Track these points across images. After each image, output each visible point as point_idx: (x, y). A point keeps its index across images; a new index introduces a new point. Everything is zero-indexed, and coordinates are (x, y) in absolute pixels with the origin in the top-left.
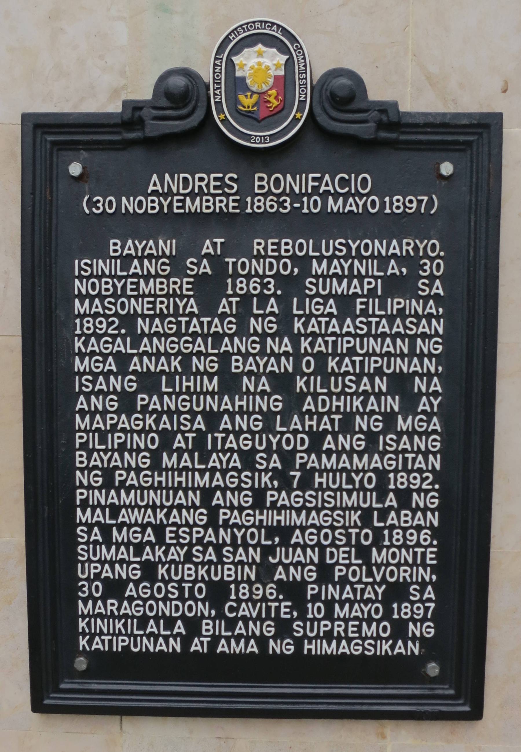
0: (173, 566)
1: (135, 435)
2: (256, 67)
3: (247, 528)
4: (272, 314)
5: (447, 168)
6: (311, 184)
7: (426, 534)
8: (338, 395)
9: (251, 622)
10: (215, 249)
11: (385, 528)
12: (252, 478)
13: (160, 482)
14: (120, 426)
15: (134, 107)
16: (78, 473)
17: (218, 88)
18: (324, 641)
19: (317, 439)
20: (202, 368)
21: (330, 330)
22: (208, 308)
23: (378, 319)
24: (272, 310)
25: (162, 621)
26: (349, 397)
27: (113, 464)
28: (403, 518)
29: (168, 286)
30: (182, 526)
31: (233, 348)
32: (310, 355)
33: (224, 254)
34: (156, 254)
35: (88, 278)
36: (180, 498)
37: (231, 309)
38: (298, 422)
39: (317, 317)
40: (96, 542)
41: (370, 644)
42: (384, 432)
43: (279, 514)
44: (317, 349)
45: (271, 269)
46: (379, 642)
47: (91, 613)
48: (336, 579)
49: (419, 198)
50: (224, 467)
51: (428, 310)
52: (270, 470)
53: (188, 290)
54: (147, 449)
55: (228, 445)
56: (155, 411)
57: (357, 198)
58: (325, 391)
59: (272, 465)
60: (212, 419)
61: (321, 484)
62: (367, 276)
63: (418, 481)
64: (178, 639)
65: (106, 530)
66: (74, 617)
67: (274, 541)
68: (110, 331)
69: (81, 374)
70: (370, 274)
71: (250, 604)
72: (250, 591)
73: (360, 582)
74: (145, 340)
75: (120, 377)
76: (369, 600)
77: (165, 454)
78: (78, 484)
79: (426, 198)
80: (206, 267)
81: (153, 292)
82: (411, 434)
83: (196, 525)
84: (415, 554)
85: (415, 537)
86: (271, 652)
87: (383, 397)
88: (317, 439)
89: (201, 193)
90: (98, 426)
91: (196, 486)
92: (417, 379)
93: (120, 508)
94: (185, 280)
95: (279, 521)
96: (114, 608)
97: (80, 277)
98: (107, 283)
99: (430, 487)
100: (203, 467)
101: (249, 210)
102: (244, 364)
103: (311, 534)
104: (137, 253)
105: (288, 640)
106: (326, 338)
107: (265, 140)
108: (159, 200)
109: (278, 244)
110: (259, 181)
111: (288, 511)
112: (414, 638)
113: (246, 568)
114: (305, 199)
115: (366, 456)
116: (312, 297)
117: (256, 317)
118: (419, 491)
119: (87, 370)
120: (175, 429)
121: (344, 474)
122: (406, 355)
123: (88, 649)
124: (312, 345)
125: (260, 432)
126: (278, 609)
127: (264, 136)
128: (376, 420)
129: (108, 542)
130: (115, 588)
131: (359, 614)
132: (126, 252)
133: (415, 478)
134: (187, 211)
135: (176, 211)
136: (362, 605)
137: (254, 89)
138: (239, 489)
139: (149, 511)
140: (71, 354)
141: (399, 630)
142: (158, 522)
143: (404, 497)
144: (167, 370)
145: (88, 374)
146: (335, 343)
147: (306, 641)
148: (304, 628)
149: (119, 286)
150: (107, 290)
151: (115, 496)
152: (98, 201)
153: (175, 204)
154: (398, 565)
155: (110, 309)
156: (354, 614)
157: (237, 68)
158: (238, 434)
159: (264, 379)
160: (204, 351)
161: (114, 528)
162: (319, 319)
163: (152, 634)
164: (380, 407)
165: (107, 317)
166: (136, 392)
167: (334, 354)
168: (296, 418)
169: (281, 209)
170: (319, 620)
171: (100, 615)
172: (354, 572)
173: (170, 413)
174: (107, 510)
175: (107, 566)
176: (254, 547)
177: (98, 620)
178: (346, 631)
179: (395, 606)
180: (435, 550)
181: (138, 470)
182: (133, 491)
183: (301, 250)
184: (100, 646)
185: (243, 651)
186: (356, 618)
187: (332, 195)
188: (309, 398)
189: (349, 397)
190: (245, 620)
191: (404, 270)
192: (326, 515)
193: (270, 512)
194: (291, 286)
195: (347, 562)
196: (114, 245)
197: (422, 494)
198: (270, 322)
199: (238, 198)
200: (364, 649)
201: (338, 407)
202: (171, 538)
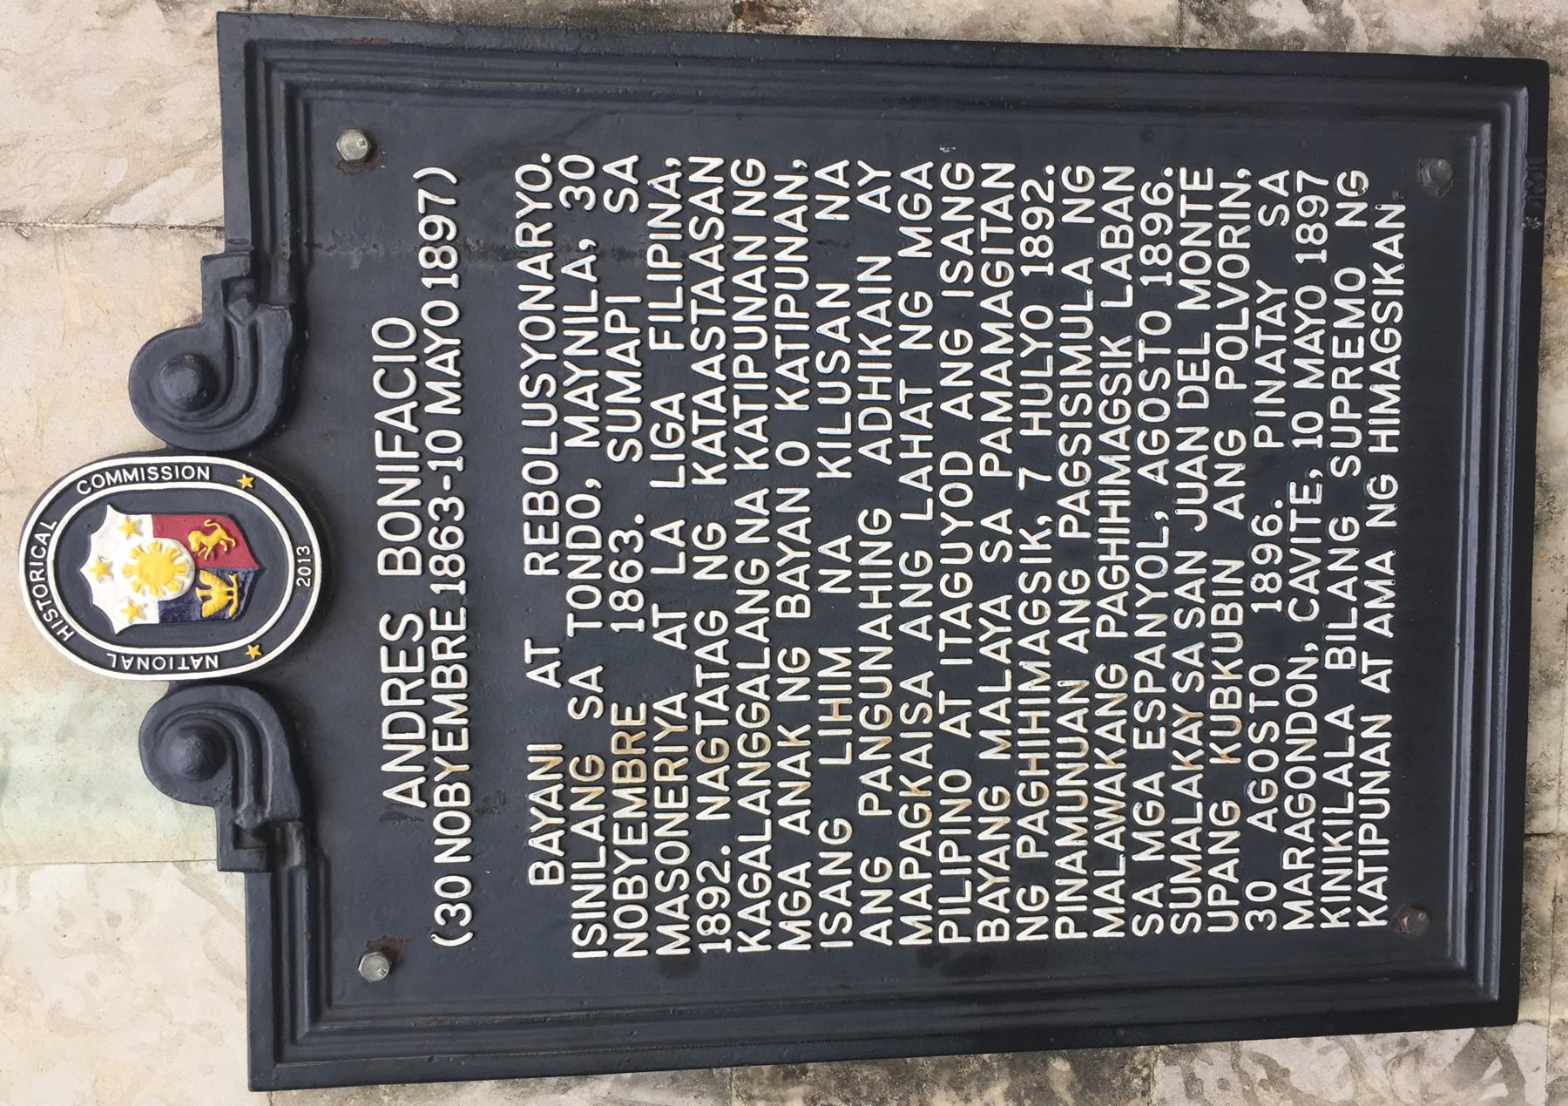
0: (1213, 733)
1: (943, 819)
2: (135, 577)
3: (1135, 578)
4: (685, 534)
5: (352, 145)
6: (397, 453)
8: (858, 388)
9: (1331, 568)
10: (549, 659)
12: (1032, 570)
13: (1041, 764)
14: (923, 851)
16: (1022, 937)
17: (188, 663)
18: (1372, 410)
19: (949, 434)
20: (804, 681)
21: (718, 407)
22: (675, 671)
23: (694, 302)
24: (676, 533)
25: (1327, 755)
26: (861, 366)
27: (1002, 865)
28: (1117, 245)
29: (627, 758)
30: (1130, 717)
31: (760, 616)
33: (559, 640)
34: (560, 787)
35: (612, 929)
36: (1071, 720)
37: (676, 622)
39: (689, 437)
40: (1165, 896)
41: (1381, 313)
44: (759, 436)
45: (589, 538)
46: (1376, 292)
47: (1310, 903)
48: (1243, 386)
49: (421, 209)
50: (1008, 629)
52: (1015, 530)
53: (635, 716)
54: (971, 794)
55: (963, 623)
56: (892, 779)
57: (427, 350)
58: (848, 416)
60: (908, 656)
61: (1043, 424)
62: (599, 327)
63: (1038, 211)
64: (1363, 719)
65: (1139, 876)
66: (1317, 938)
67: (1163, 522)
68: (726, 880)
70: (594, 320)
71: (1293, 570)
73: (1248, 336)
75: (823, 855)
76: (1288, 315)
77: (983, 756)
78: (1045, 937)
79: (422, 194)
80: (588, 678)
81: (643, 790)
82: (941, 230)
83: (1128, 688)
84: (1192, 216)
85: (1157, 217)
86: (1393, 524)
87: (861, 290)
88: (949, 434)
89: (425, 692)
91: (1047, 688)
92: (821, 215)
93: (1094, 849)
94: (614, 722)
95: (1121, 512)
96: (1300, 855)
97: (611, 946)
98: (623, 889)
99: (1051, 184)
100: (1008, 674)
101: (461, 588)
102: (793, 591)
103: (1147, 443)
105: (1370, 487)
106: (737, 415)
107: (304, 555)
108: (442, 782)
109: (534, 522)
110: (395, 568)
111: (1101, 493)
112: (1371, 215)
114: (433, 465)
115: (984, 326)
116: (649, 448)
117: (692, 567)
118: (1058, 209)
119: (808, 923)
120: (929, 735)
121: (1024, 373)
122: (770, 240)
123: (1385, 908)
124: (750, 445)
126: (1303, 511)
128: (909, 304)
129: (1162, 871)
130: (1259, 854)
131: (1316, 335)
132: (555, 850)
134: (464, 721)
136: (1297, 331)
137: (188, 582)
138: (1054, 597)
141: (1352, 248)
142: (1123, 766)
143: (1072, 242)
145: (815, 921)
146: (746, 397)
147: (1372, 449)
148: (1344, 453)
149: (629, 862)
150: (637, 888)
151: (1068, 859)
152: (445, 914)
153: (450, 747)
154: (1215, 253)
155: (679, 879)
157: (138, 621)
158: (942, 603)
159: (824, 549)
160: (767, 677)
161: (1136, 858)
162: (695, 431)
163: (1353, 775)
164: (882, 298)
167: (770, 398)
169: (457, 518)
170: (1329, 422)
171: (1315, 885)
173: (897, 747)
174: (1097, 873)
176: (1175, 562)
177: (1324, 888)
178: (1351, 364)
179: (1300, 258)
180: (1183, 172)
181: (1016, 811)
182: (1059, 821)
183: (545, 473)
184: (1379, 882)
185: (1389, 582)
186: (1326, 343)
187: (421, 405)
188: (864, 451)
189: (861, 366)
190: (1325, 579)
191: (584, 244)
193: (1102, 530)
194: (626, 493)
195: (1206, 363)
197: (1066, 202)
198: (702, 537)
199: (433, 612)
201: (882, 388)
202: (1156, 740)
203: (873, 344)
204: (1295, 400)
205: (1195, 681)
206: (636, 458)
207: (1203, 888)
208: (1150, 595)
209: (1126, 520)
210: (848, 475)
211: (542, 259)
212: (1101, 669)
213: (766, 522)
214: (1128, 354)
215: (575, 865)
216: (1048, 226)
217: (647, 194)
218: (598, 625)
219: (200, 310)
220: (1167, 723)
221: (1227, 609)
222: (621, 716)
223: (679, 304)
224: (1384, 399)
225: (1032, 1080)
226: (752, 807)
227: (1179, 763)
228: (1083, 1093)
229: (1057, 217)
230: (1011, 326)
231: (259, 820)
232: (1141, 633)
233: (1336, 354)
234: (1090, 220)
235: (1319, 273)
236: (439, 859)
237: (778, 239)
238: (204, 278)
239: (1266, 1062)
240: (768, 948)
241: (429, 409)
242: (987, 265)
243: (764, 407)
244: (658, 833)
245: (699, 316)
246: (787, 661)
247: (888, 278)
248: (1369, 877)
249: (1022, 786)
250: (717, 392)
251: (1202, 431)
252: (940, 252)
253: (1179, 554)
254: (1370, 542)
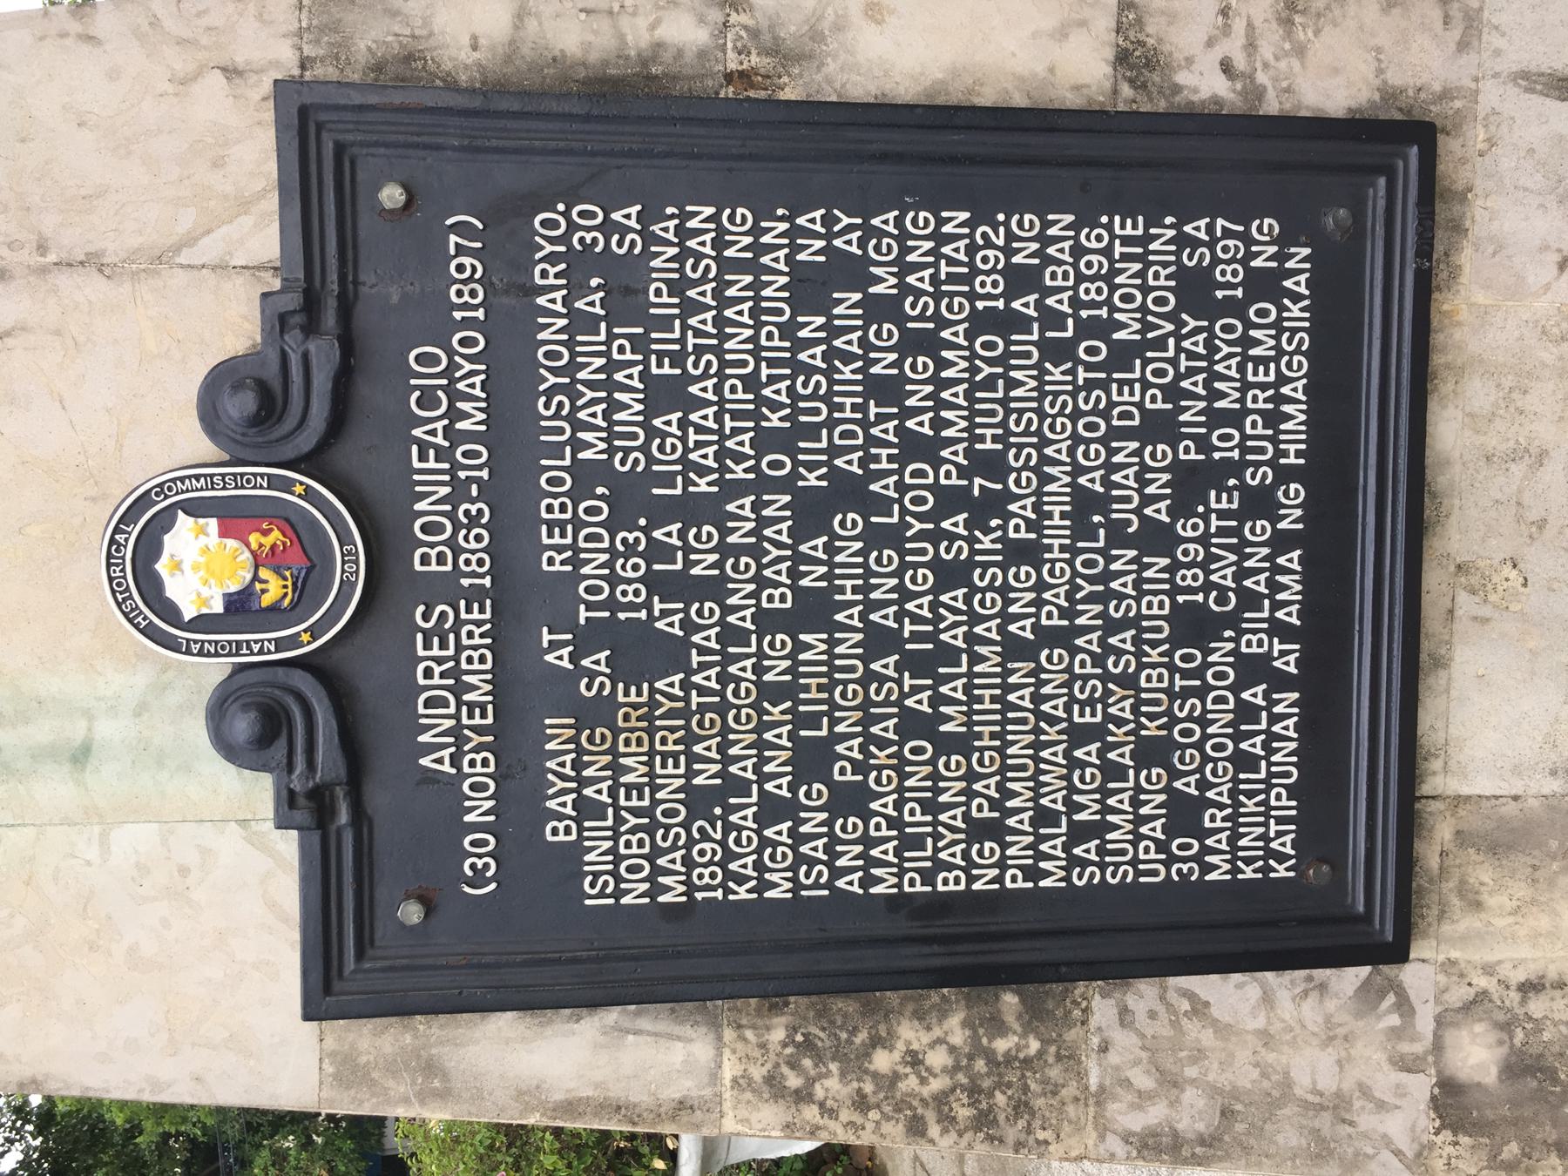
0: (1144, 709)
1: (908, 783)
2: (202, 573)
4: (682, 535)
5: (392, 195)
6: (432, 464)
7: (1088, 237)
8: (833, 407)
9: (1246, 564)
10: (565, 644)
11: (1076, 316)
12: (985, 566)
13: (993, 736)
14: (890, 811)
15: (289, 808)
16: (977, 886)
18: (1282, 427)
19: (914, 448)
20: (786, 664)
21: (711, 424)
22: (674, 654)
23: (690, 333)
24: (675, 534)
25: (1243, 727)
26: (836, 388)
27: (959, 824)
28: (1059, 283)
29: (632, 730)
30: (1071, 694)
31: (748, 607)
32: (758, 462)
33: (573, 627)
34: (573, 755)
35: (618, 879)
37: (676, 612)
38: (883, 482)
39: (686, 450)
40: (1101, 851)
41: (1290, 342)
42: (900, 319)
43: (1050, 515)
44: (747, 450)
45: (599, 538)
46: (1286, 324)
47: (1228, 857)
48: (1170, 406)
49: (452, 252)
50: (965, 618)
51: (670, 236)
53: (639, 694)
54: (932, 762)
55: (926, 613)
56: (863, 749)
57: (457, 375)
58: (825, 432)
59: (961, 531)
60: (878, 641)
61: (995, 439)
62: (607, 354)
63: (991, 253)
64: (1275, 696)
65: (1079, 833)
66: (1234, 888)
67: (1100, 525)
68: (718, 836)
69: (797, 886)
70: (603, 348)
71: (1213, 567)
72: (1189, 566)
73: (1174, 362)
74: (733, 769)
75: (802, 815)
76: (1208, 344)
77: (942, 728)
78: (996, 886)
79: (453, 238)
81: (645, 758)
82: (905, 269)
83: (1069, 669)
84: (1125, 257)
85: (1094, 258)
86: (1301, 526)
87: (836, 322)
88: (914, 448)
89: (456, 673)
90: (891, 852)
91: (998, 669)
92: (801, 257)
94: (621, 699)
95: (1063, 516)
96: (1219, 815)
97: (618, 894)
98: (628, 845)
99: (1002, 229)
100: (964, 657)
101: (487, 581)
102: (777, 585)
103: (1086, 455)
104: (571, 791)
105: (1280, 494)
106: (728, 432)
107: (349, 553)
108: (470, 751)
109: (551, 525)
110: (429, 564)
111: (1046, 499)
112: (1281, 257)
113: (1148, 574)
114: (462, 475)
115: (944, 354)
116: (651, 460)
117: (689, 564)
118: (1008, 252)
119: (789, 874)
120: (896, 710)
121: (978, 395)
122: (757, 278)
123: (1293, 861)
124: (739, 458)
125: (902, 554)
126: (1222, 515)
127: (343, 555)
128: (878, 334)
129: (1098, 829)
130: (1184, 815)
131: (1234, 362)
132: (569, 811)
133: (985, 260)
134: (490, 698)
135: (490, 720)
136: (1217, 357)
137: (249, 577)
138: (1005, 589)
139: (1045, 754)
140: (761, 906)
141: (1265, 285)
142: (1065, 737)
143: (1020, 280)
144: (789, 727)
145: (796, 873)
146: (735, 416)
147: (1282, 461)
149: (633, 821)
150: (641, 844)
151: (1017, 818)
152: (473, 866)
153: (477, 721)
154: (1145, 290)
155: (677, 835)
156: (1233, 373)
157: (205, 611)
158: (906, 595)
159: (804, 548)
160: (754, 660)
161: (1076, 817)
162: (691, 445)
163: (1265, 745)
164: (855, 329)
165: (691, 843)
166: (830, 783)
167: (756, 416)
168: (874, 487)
169: (484, 521)
170: (1245, 437)
172: (1156, 373)
173: (868, 721)
174: (1042, 831)
175: (1144, 830)
176: (1110, 560)
177: (1240, 843)
178: (1263, 387)
179: (1219, 294)
180: (1117, 219)
181: (971, 777)
182: (1009, 785)
183: (561, 482)
184: (1288, 838)
185: (1297, 577)
186: (1241, 368)
187: (452, 423)
188: (839, 462)
189: (836, 388)
190: (1241, 574)
192: (1052, 428)
193: (1046, 532)
194: (631, 499)
195: (1137, 386)
196: (557, 833)
197: (1015, 245)
198: (697, 538)
199: (463, 603)
200: (1297, 351)
201: (855, 408)
202: (1093, 714)
203: (847, 370)
204: (1215, 418)
205: (1128, 663)
206: (639, 469)
207: (1135, 844)
208: (1088, 588)
209: (1067, 523)
210: (824, 483)
211: (558, 295)
212: (1046, 652)
213: (753, 524)
214: (1069, 378)
215: (587, 824)
216: (1000, 267)
217: (650, 239)
218: (607, 614)
219: (259, 339)
220: (1103, 700)
221: (1156, 600)
222: (626, 694)
223: (677, 335)
224: (1292, 417)
225: (986, 1012)
226: (741, 773)
227: (1114, 734)
228: (1030, 1022)
229: (1008, 259)
230: (967, 353)
231: (311, 784)
232: (1081, 621)
233: (1250, 378)
234: (1037, 261)
235: (1236, 308)
236: (467, 818)
237: (764, 278)
238: (263, 312)
239: (1189, 995)
240: (755, 896)
241: (459, 426)
242: (946, 300)
243: (751, 424)
244: (659, 796)
245: (695, 345)
246: (772, 645)
247: (860, 312)
249: (977, 755)
250: (711, 411)
251: (1134, 445)
252: (905, 289)
253: (1114, 552)
254: (1281, 542)
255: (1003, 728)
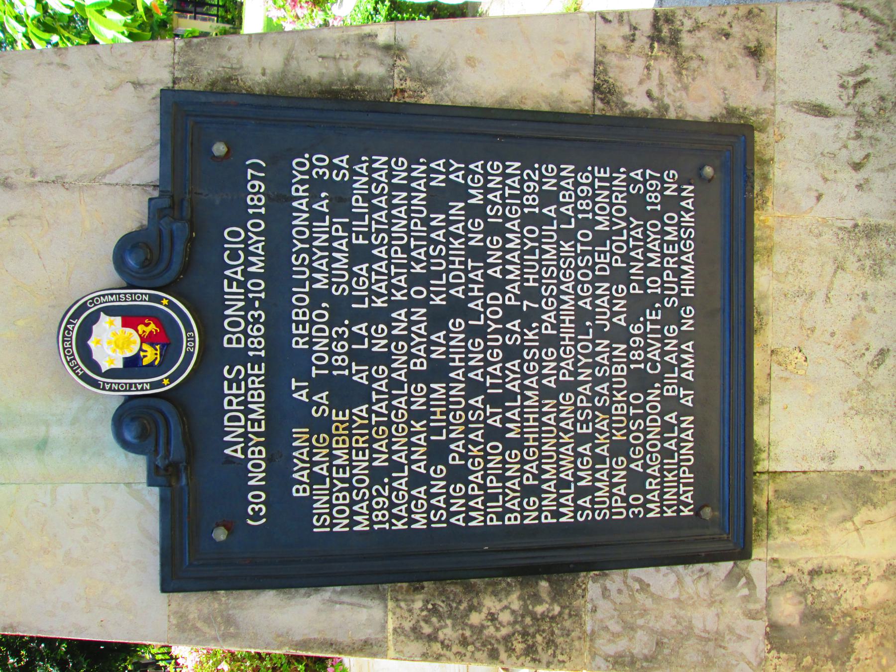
0: (614, 425)
1: (489, 465)
3: (577, 353)
4: (368, 330)
5: (220, 149)
6: (234, 290)
10: (304, 388)
13: (534, 440)
14: (480, 481)
16: (526, 522)
17: (136, 387)
18: (682, 277)
19: (491, 285)
20: (424, 400)
21: (384, 270)
22: (363, 395)
23: (373, 222)
25: (665, 435)
26: (450, 252)
27: (517, 487)
28: (567, 200)
29: (340, 435)
30: (575, 417)
33: (308, 378)
36: (549, 419)
37: (364, 371)
38: (476, 303)
39: (371, 284)
40: (592, 502)
41: (685, 233)
42: (485, 217)
43: (564, 321)
44: (403, 284)
45: (323, 331)
46: (683, 224)
49: (249, 178)
50: (519, 376)
51: (364, 172)
52: (522, 330)
53: (344, 415)
54: (502, 454)
56: (465, 446)
57: (250, 242)
58: (444, 275)
59: (517, 329)
60: (473, 388)
61: (534, 280)
62: (329, 232)
63: (531, 184)
64: (682, 418)
65: (580, 493)
66: (663, 521)
67: (589, 327)
68: (386, 494)
69: (430, 522)
70: (327, 229)
72: (636, 349)
73: (627, 242)
74: (395, 457)
76: (644, 233)
77: (507, 436)
78: (537, 521)
79: (250, 171)
80: (322, 397)
81: (347, 451)
82: (487, 191)
83: (575, 403)
84: (600, 188)
85: (585, 188)
87: (451, 218)
88: (491, 285)
89: (245, 403)
91: (537, 404)
92: (433, 184)
93: (559, 479)
94: (334, 418)
95: (571, 321)
96: (654, 482)
98: (337, 498)
99: (537, 172)
100: (519, 397)
101: (263, 353)
102: (419, 357)
105: (682, 311)
106: (393, 274)
107: (191, 337)
109: (298, 323)
110: (231, 343)
111: (561, 313)
112: (680, 190)
113: (615, 353)
114: (251, 295)
115: (508, 235)
116: (352, 289)
119: (425, 515)
120: (482, 425)
121: (526, 257)
122: (409, 194)
123: (692, 506)
124: (399, 289)
126: (653, 322)
128: (473, 224)
129: (591, 490)
130: (636, 482)
131: (657, 243)
132: (305, 479)
133: (529, 187)
134: (263, 417)
135: (263, 429)
136: (648, 240)
138: (540, 361)
139: (562, 450)
141: (672, 204)
146: (397, 266)
147: (682, 295)
148: (670, 296)
149: (340, 485)
150: (344, 498)
152: (253, 509)
153: (256, 429)
154: (611, 205)
155: (364, 494)
158: (488, 363)
159: (433, 337)
160: (406, 398)
161: (579, 484)
162: (373, 281)
163: (677, 444)
164: (460, 221)
165: (372, 497)
170: (663, 282)
171: (661, 496)
173: (468, 431)
175: (615, 490)
178: (672, 256)
179: (649, 208)
180: (596, 168)
182: (543, 466)
183: (303, 300)
188: (452, 292)
189: (450, 252)
190: (663, 354)
191: (323, 195)
194: (341, 310)
195: (608, 254)
196: (299, 492)
197: (544, 180)
198: (376, 331)
199: (249, 365)
201: (460, 263)
202: (588, 428)
203: (456, 243)
204: (648, 272)
205: (605, 401)
206: (345, 294)
207: (610, 498)
208: (584, 360)
209: (573, 325)
210: (444, 303)
211: (304, 201)
212: (562, 395)
213: (406, 324)
214: (573, 249)
215: (315, 487)
216: (536, 191)
217: (353, 173)
218: (327, 372)
219: (145, 222)
220: (593, 420)
221: (619, 367)
222: (337, 415)
223: (366, 223)
224: (687, 272)
225: (531, 591)
226: (399, 460)
227: (598, 439)
228: (555, 597)
229: (540, 187)
230: (519, 235)
231: (167, 462)
232: (581, 378)
233: (665, 251)
234: (555, 189)
235: (659, 215)
236: (250, 483)
237: (413, 194)
238: (149, 208)
239: (639, 581)
240: (406, 527)
241: (250, 269)
242: (508, 208)
243: (405, 271)
244: (354, 472)
245: (376, 229)
246: (416, 390)
247: (463, 212)
248: (685, 492)
249: (526, 450)
250: (384, 263)
251: (607, 285)
252: (487, 201)
253: (597, 341)
254: (683, 337)
255: (540, 435)
